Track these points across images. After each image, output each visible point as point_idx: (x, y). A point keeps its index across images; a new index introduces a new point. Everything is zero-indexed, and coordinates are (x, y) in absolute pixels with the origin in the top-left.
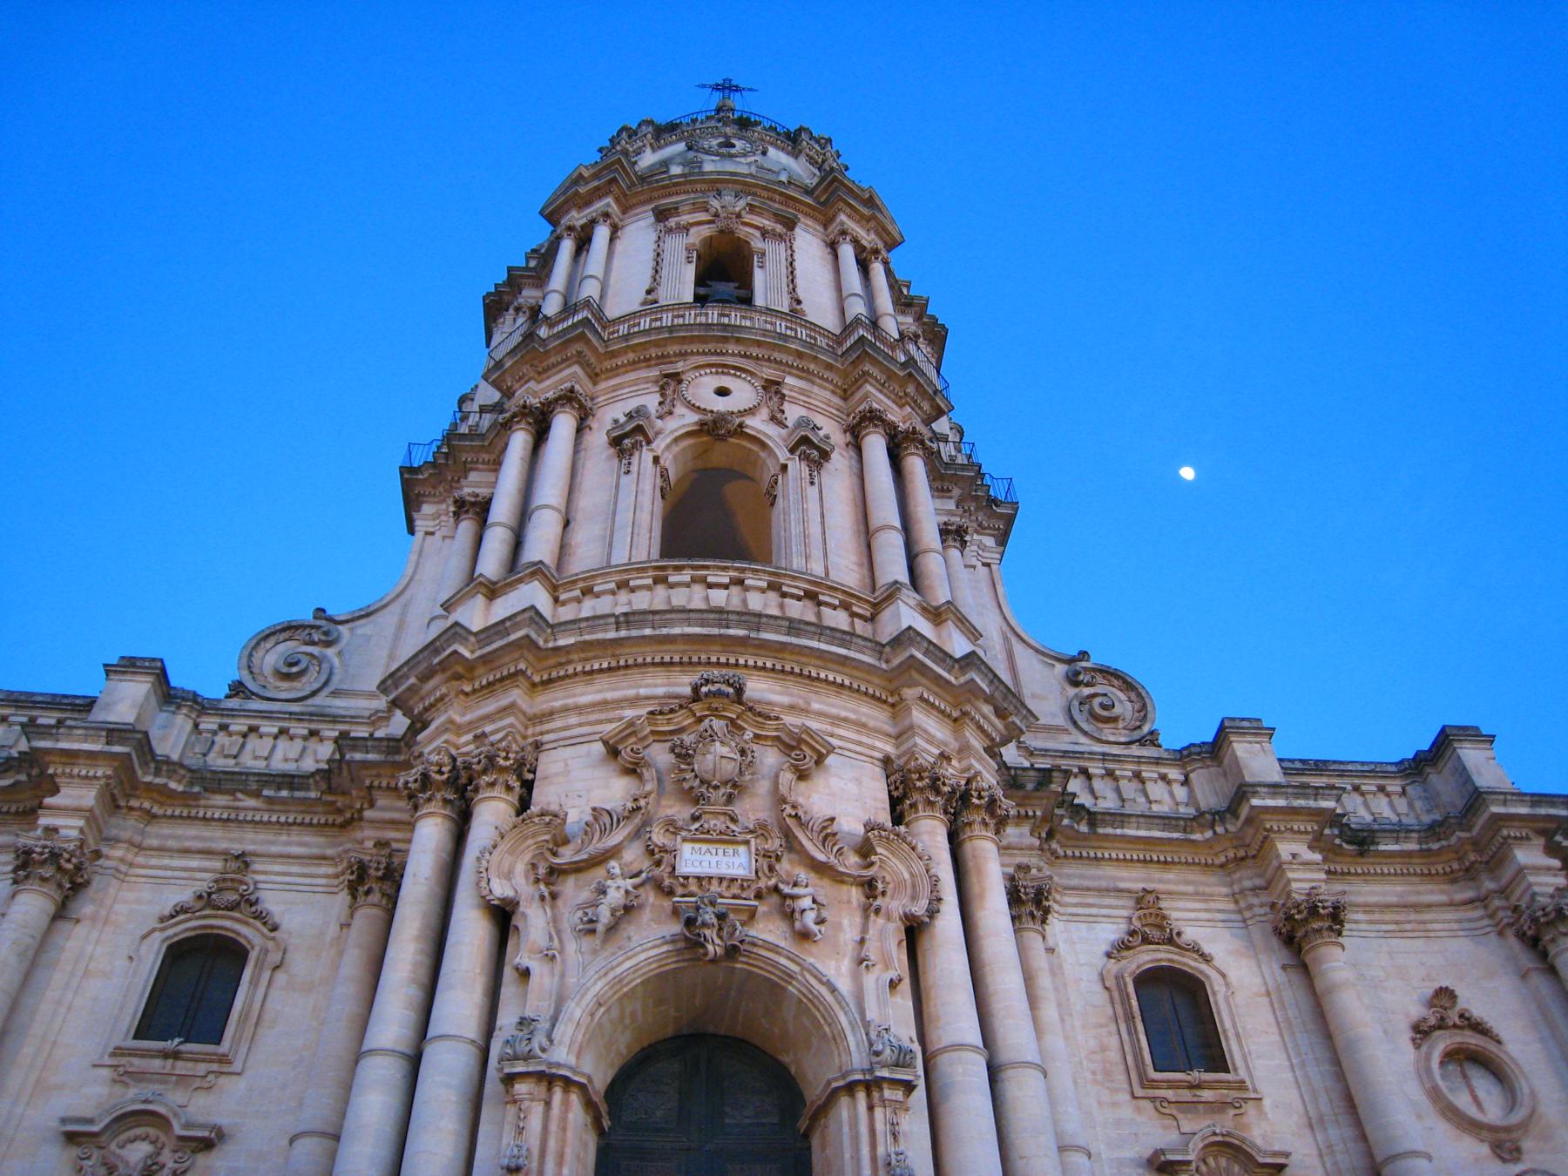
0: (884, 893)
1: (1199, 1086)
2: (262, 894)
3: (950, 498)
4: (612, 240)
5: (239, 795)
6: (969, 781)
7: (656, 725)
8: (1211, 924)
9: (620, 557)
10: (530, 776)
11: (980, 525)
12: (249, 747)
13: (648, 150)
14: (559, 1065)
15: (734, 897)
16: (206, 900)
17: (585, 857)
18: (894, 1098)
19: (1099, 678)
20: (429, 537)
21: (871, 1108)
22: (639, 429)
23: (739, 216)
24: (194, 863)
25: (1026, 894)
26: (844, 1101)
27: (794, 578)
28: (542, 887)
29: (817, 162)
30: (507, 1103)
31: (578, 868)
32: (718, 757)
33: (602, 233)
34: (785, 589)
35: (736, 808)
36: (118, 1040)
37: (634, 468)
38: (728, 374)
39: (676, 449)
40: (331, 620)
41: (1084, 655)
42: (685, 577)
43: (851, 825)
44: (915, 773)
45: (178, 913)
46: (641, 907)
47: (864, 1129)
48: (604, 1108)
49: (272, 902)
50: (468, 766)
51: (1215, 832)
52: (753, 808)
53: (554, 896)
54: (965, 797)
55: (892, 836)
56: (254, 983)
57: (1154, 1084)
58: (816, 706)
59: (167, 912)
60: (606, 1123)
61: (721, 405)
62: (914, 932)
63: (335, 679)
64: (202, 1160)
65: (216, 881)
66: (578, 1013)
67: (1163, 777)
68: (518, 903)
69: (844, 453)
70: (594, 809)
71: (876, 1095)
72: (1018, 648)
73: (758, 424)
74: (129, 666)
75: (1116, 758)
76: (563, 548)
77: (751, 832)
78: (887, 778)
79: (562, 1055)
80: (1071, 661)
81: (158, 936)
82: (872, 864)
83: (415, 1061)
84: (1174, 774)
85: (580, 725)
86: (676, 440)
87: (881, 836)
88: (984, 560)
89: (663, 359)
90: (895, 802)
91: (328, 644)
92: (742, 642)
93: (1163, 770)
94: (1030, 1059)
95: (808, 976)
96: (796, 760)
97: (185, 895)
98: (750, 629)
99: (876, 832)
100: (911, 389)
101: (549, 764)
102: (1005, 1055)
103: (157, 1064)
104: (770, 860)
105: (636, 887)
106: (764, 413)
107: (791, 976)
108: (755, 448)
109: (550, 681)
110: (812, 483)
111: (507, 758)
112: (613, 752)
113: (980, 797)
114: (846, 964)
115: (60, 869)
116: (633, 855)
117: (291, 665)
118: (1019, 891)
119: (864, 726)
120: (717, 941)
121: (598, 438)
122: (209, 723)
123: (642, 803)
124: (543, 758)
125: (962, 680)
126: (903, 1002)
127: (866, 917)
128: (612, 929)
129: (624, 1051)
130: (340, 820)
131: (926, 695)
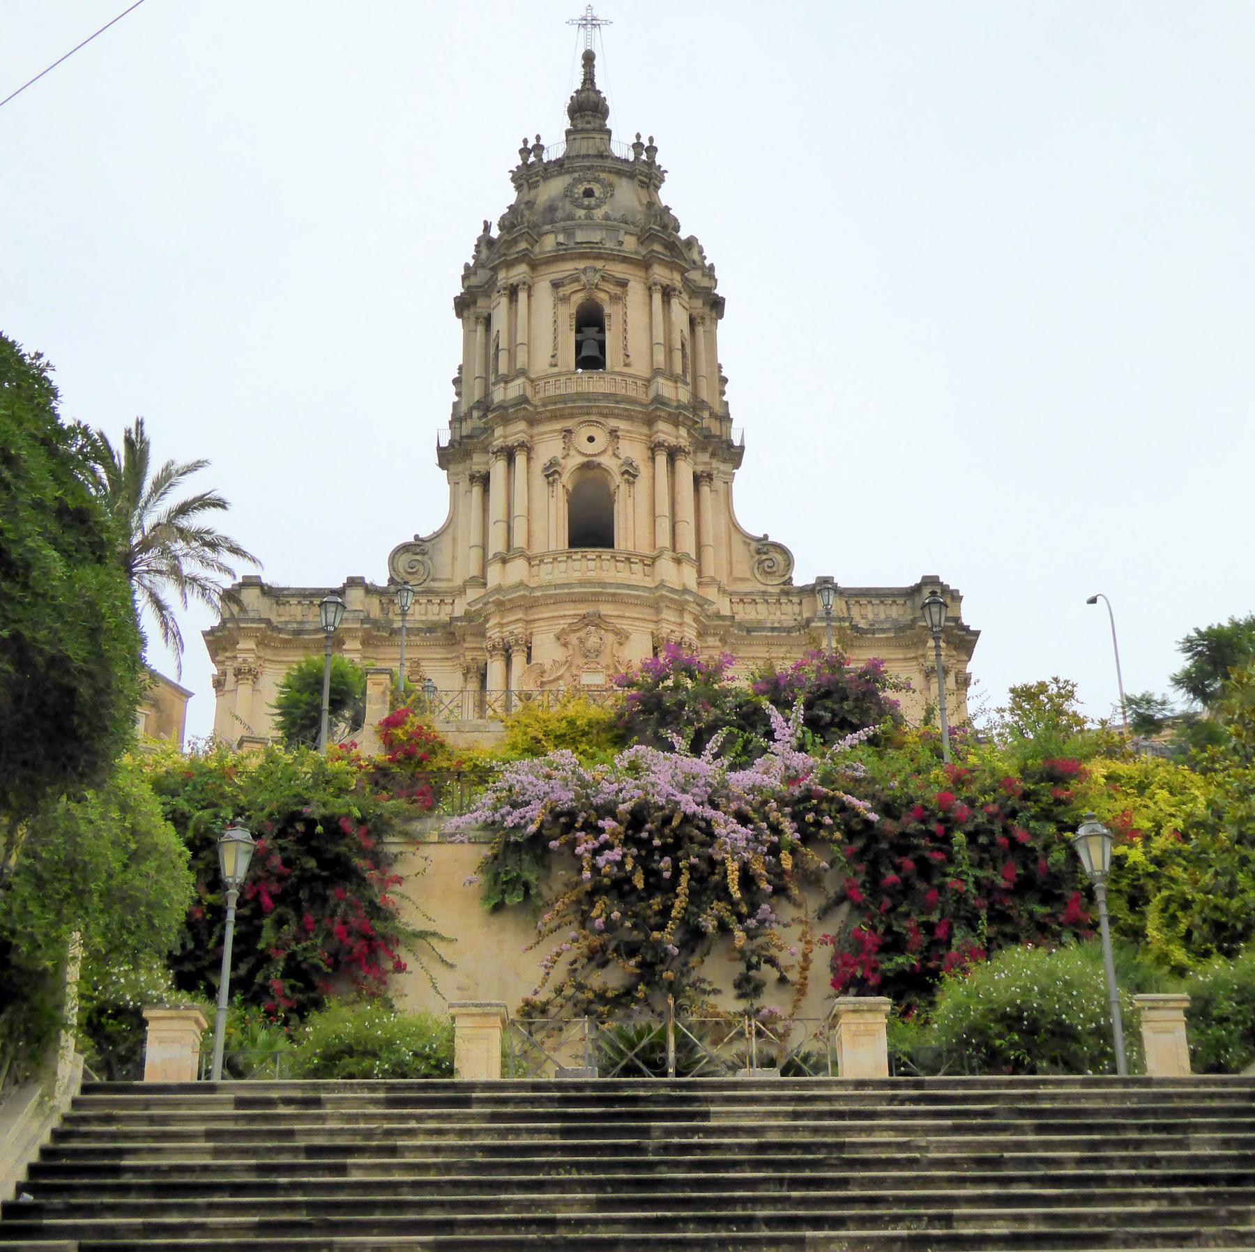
4: (529, 296)
9: (552, 547)
13: (541, 181)
19: (771, 548)
29: (645, 183)
32: (593, 641)
33: (522, 296)
37: (555, 494)
40: (422, 540)
41: (766, 537)
42: (578, 556)
50: (509, 642)
52: (605, 659)
54: (680, 644)
58: (627, 614)
72: (735, 537)
73: (607, 461)
74: (353, 582)
80: (759, 540)
84: (795, 600)
90: (655, 648)
91: (424, 554)
92: (601, 594)
101: (536, 641)
106: (610, 452)
108: (606, 473)
112: (558, 639)
116: (567, 675)
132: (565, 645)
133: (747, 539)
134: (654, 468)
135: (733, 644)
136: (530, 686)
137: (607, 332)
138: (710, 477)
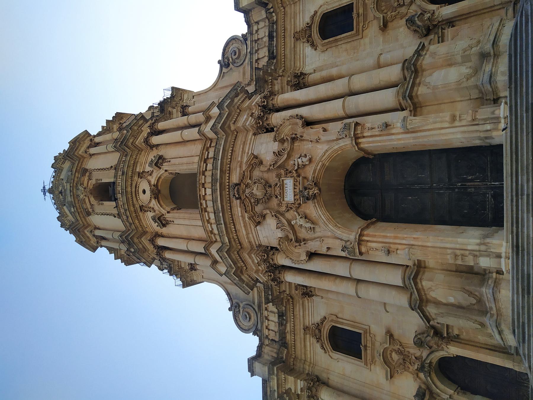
0: (296, 134)
1: (358, 14)
2: (316, 323)
3: (172, 111)
4: (99, 229)
5: (286, 331)
6: (259, 106)
7: (250, 210)
8: (304, 11)
9: (200, 223)
10: (269, 248)
11: (180, 100)
12: (273, 328)
14: (355, 238)
15: (300, 184)
16: (319, 339)
17: (291, 231)
18: (360, 129)
20: (204, 277)
21: (364, 137)
22: (159, 218)
23: (85, 188)
24: (308, 344)
25: (296, 82)
26: (362, 146)
27: (200, 167)
28: (302, 244)
30: (368, 254)
31: (295, 233)
32: (257, 191)
33: (98, 233)
34: (204, 170)
35: (273, 184)
36: (363, 364)
38: (138, 190)
39: (164, 206)
40: (232, 306)
41: (219, 62)
43: (276, 146)
44: (258, 125)
45: (323, 348)
46: (305, 213)
47: (371, 139)
48: (369, 221)
49: (317, 319)
51: (273, 12)
52: (272, 178)
53: (304, 240)
54: (264, 107)
55: (278, 133)
56: (342, 323)
57: (358, 31)
59: (324, 351)
60: (374, 220)
61: (148, 192)
62: (308, 123)
63: (249, 303)
64: (395, 337)
65: (313, 337)
66: (339, 232)
67: (257, 31)
68: (307, 251)
69: (160, 149)
70: (277, 228)
71: (359, 135)
73: (153, 181)
75: (252, 48)
76: (200, 240)
77: (279, 179)
78: (260, 134)
79: (352, 236)
81: (331, 353)
82: (287, 138)
83: (359, 281)
85: (252, 233)
86: (161, 206)
87: (278, 136)
88: (192, 98)
89: (135, 211)
93: (254, 32)
94: (347, 81)
95: (323, 159)
96: (256, 166)
97: (318, 346)
98: (217, 182)
99: (277, 138)
100: (136, 128)
101: (264, 242)
102: (346, 90)
103: (369, 352)
104: (288, 173)
105: (299, 215)
106: (149, 178)
107: (323, 165)
108: (161, 180)
109: (240, 243)
110: (170, 161)
111: (264, 256)
112: (259, 223)
113: (264, 102)
114: (319, 146)
115: (313, 386)
117: (246, 317)
118: (295, 84)
119: (244, 142)
120: (313, 189)
121: (163, 231)
122: (267, 342)
123: (273, 214)
124: (263, 244)
125: (227, 110)
126: (330, 126)
127: (304, 140)
128: (313, 223)
129: (351, 215)
130: (291, 300)
131: (233, 122)
132: (264, 217)
133: (221, 75)
134: (162, 144)
135: (283, 71)
136: (301, 252)
137: (103, 181)
138: (184, 107)
